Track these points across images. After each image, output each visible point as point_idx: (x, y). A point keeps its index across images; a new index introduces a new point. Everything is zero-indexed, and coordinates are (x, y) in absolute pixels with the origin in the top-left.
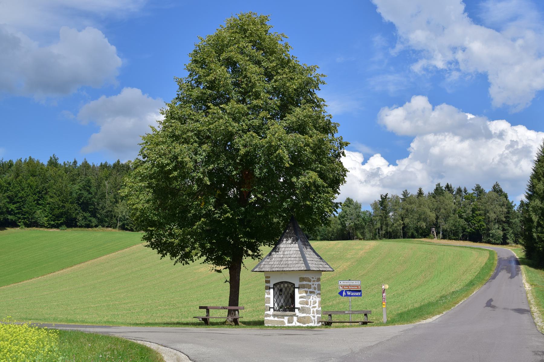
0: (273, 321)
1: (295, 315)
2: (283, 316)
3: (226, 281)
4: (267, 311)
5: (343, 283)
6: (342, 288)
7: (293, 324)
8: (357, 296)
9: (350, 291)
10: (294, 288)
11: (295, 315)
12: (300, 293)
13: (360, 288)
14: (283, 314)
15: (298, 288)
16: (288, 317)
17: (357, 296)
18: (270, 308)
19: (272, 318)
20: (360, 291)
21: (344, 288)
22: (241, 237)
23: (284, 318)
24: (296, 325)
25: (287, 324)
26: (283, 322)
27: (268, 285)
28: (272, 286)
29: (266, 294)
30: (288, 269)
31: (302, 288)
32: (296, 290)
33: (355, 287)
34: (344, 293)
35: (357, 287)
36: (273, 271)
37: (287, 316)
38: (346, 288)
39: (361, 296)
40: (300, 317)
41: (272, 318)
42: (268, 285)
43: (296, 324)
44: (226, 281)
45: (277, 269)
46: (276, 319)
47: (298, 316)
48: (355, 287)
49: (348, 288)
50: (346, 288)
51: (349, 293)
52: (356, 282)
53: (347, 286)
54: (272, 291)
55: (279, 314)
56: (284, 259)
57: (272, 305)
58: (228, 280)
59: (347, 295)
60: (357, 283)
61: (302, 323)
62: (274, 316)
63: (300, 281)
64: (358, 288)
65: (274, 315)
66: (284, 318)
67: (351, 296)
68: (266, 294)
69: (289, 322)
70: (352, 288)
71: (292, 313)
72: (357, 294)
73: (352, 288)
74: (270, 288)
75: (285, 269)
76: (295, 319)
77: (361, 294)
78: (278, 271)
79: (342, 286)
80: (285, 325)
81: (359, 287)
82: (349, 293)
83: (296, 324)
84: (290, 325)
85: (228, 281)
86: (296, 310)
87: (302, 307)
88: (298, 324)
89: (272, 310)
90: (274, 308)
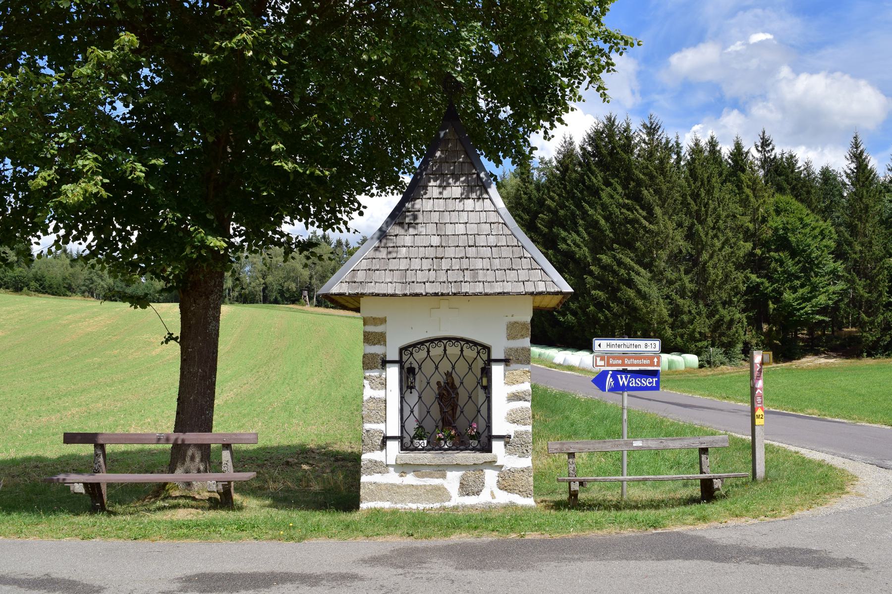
0: (399, 487)
1: (491, 464)
2: (441, 470)
3: (170, 338)
4: (371, 450)
5: (609, 349)
6: (602, 363)
7: (484, 498)
8: (646, 388)
9: (624, 372)
10: (490, 361)
11: (491, 464)
12: (510, 382)
13: (658, 365)
14: (443, 462)
15: (506, 361)
16: (460, 474)
17: (646, 388)
18: (386, 439)
19: (392, 477)
20: (655, 374)
21: (609, 365)
22: (277, 155)
23: (444, 477)
24: (494, 501)
25: (456, 499)
26: (440, 493)
27: (377, 349)
28: (393, 355)
29: (367, 386)
30: (479, 288)
31: (519, 361)
32: (497, 371)
33: (645, 362)
34: (609, 381)
35: (648, 362)
36: (417, 295)
37: (457, 467)
38: (616, 362)
39: (657, 388)
40: (511, 472)
41: (392, 477)
42: (377, 349)
43: (493, 496)
44: (170, 338)
45: (430, 289)
46: (410, 479)
47: (502, 467)
48: (645, 362)
49: (623, 364)
50: (616, 362)
51: (623, 381)
52: (646, 346)
53: (618, 358)
54: (393, 373)
55: (426, 462)
56: (450, 252)
57: (394, 429)
58: (177, 333)
59: (617, 388)
60: (649, 349)
61: (520, 493)
62: (403, 468)
63: (511, 337)
64: (652, 364)
65: (402, 465)
66: (444, 477)
67: (629, 388)
68: (367, 386)
69: (466, 489)
70: (635, 362)
71: (481, 457)
72: (646, 382)
73: (635, 362)
74: (385, 363)
75: (466, 288)
76: (491, 476)
77: (657, 383)
78: (436, 294)
79: (602, 359)
80: (447, 504)
81: (656, 360)
82: (623, 381)
83: (493, 496)
84: (470, 500)
85: (176, 339)
86: (497, 446)
87: (518, 435)
88: (503, 498)
89: (393, 446)
90: (401, 438)
